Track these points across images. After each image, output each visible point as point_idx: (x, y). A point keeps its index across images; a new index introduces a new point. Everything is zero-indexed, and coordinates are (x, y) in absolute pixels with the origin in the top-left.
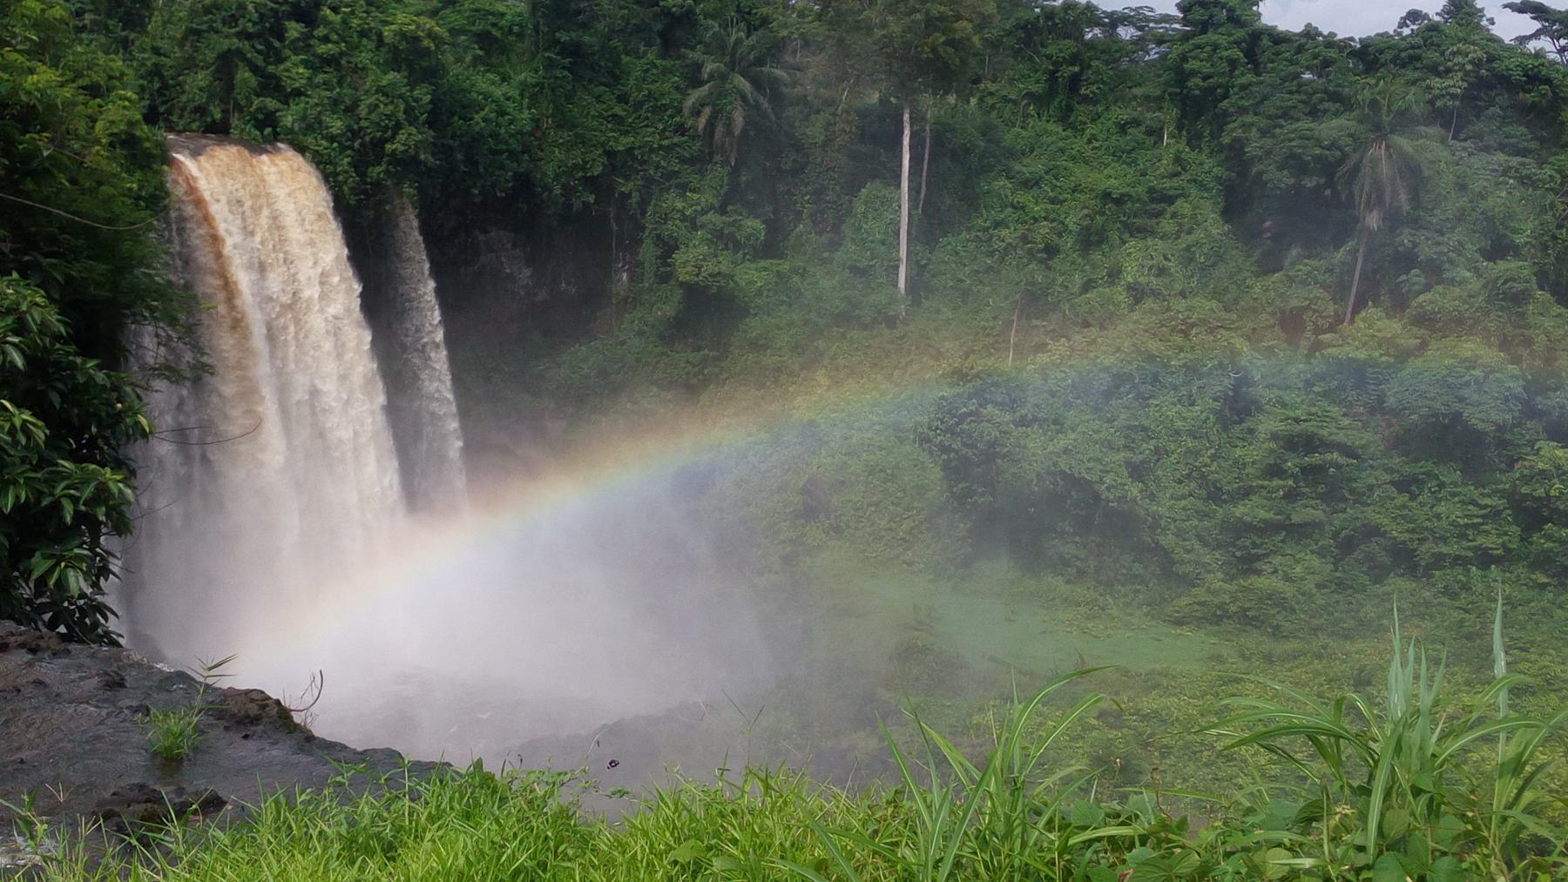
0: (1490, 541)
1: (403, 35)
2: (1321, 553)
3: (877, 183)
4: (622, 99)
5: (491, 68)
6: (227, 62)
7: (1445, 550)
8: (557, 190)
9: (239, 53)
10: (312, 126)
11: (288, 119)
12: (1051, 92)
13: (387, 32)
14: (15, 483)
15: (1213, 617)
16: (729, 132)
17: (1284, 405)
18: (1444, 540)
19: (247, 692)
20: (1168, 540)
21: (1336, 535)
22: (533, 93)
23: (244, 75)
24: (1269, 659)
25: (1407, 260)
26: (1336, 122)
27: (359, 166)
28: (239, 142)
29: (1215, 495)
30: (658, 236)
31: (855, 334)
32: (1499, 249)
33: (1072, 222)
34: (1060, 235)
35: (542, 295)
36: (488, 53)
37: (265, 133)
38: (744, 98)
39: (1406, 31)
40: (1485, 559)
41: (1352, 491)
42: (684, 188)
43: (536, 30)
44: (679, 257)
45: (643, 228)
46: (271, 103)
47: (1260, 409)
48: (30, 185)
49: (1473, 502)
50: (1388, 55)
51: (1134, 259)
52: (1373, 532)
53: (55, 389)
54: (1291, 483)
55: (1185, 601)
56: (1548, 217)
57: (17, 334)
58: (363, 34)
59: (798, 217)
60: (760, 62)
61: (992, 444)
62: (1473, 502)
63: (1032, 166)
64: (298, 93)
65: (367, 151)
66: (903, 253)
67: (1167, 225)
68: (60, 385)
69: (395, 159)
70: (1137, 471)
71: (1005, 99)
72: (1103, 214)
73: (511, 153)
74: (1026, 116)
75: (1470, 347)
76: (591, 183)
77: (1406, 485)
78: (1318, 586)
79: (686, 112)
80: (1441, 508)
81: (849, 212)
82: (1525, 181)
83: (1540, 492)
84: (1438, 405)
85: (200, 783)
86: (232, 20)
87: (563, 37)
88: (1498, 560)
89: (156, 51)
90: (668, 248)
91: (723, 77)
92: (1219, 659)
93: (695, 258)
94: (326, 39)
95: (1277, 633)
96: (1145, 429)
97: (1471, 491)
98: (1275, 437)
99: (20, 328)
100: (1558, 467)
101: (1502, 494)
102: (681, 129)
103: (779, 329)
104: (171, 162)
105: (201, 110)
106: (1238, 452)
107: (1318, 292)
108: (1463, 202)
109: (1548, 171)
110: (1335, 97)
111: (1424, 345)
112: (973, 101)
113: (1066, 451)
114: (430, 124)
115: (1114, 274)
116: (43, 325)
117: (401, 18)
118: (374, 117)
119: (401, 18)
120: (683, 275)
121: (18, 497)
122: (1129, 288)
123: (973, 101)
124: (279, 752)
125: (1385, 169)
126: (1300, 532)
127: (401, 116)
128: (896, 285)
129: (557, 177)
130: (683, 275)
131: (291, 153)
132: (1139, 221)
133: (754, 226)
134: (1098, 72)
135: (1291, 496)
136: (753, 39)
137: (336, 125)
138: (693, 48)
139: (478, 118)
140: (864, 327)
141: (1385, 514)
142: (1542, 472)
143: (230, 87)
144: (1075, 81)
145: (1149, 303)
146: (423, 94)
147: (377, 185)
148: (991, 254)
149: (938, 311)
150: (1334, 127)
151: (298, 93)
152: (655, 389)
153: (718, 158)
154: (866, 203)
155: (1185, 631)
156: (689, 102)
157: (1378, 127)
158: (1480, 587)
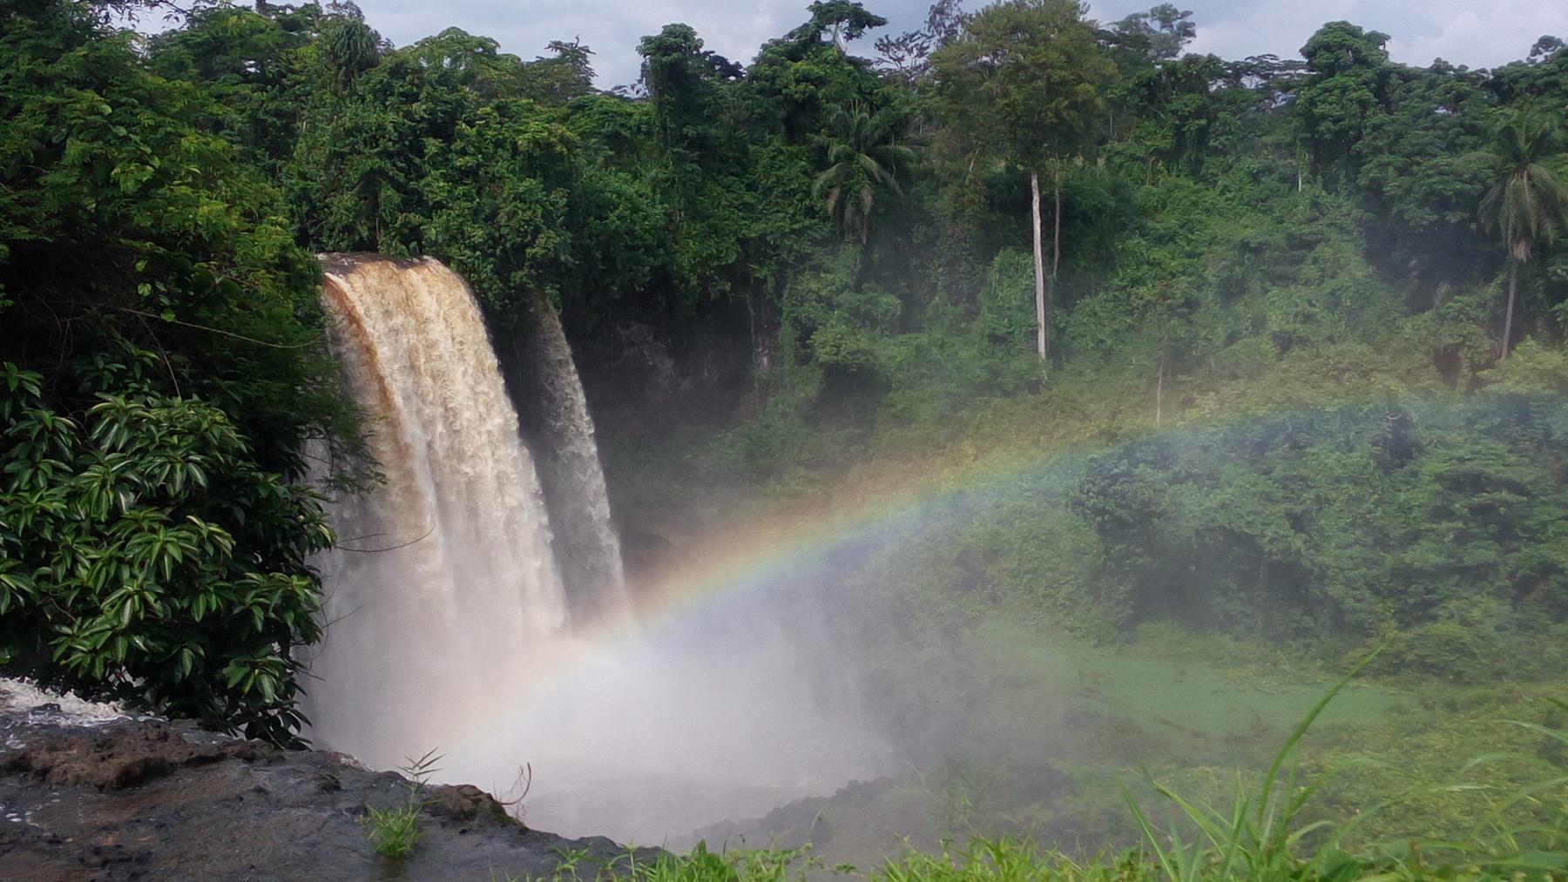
1: (537, 143)
2: (1499, 594)
3: (1010, 249)
4: (751, 187)
5: (622, 167)
6: (370, 181)
8: (694, 281)
9: (382, 172)
11: (432, 232)
12: (1179, 148)
13: (521, 141)
14: (206, 592)
15: (1393, 667)
17: (1446, 445)
20: (1337, 591)
21: (1511, 575)
22: (664, 189)
23: (387, 193)
26: (1473, 155)
27: (502, 271)
29: (1382, 541)
30: (796, 319)
31: (997, 401)
33: (1211, 274)
34: (1199, 288)
35: (686, 385)
36: (619, 154)
37: (412, 248)
38: (871, 176)
41: (1524, 529)
42: (818, 269)
43: (664, 127)
44: (817, 338)
45: (780, 312)
46: (415, 218)
47: (1421, 450)
48: (203, 312)
51: (1277, 308)
53: (241, 505)
54: (1460, 524)
55: (1359, 652)
57: (199, 453)
58: (498, 144)
59: (933, 290)
60: (885, 140)
61: (1146, 504)
63: (1170, 221)
64: (440, 206)
65: (509, 257)
66: (1041, 319)
67: (1309, 271)
68: (244, 500)
69: (536, 263)
70: (1298, 522)
71: (1134, 158)
72: (1242, 264)
74: (1155, 172)
76: (726, 271)
78: (1498, 629)
79: (815, 194)
81: (983, 282)
86: (373, 141)
87: (690, 131)
89: (303, 176)
90: (806, 331)
91: (849, 158)
92: (1399, 709)
93: (832, 338)
94: (463, 152)
95: (1459, 679)
96: (1303, 479)
98: (1439, 478)
99: (203, 446)
102: (811, 212)
103: (922, 401)
104: (320, 279)
105: (349, 229)
106: (1402, 497)
107: (1472, 328)
110: (1472, 130)
112: (1101, 162)
113: (1223, 506)
115: (1259, 325)
116: (223, 438)
117: (533, 126)
118: (512, 223)
119: (533, 126)
120: (823, 354)
121: (208, 608)
122: (1277, 336)
123: (1101, 162)
125: (1528, 197)
126: (1474, 575)
127: (539, 221)
128: (1036, 351)
129: (693, 269)
130: (823, 354)
131: (434, 265)
132: (1279, 269)
134: (1225, 124)
135: (1462, 538)
136: (877, 119)
137: (478, 234)
138: (818, 132)
139: (612, 217)
140: (1006, 394)
143: (375, 205)
144: (1203, 133)
145: (1296, 351)
146: (559, 197)
147: (521, 288)
148: (1131, 313)
149: (1080, 374)
150: (1476, 159)
151: (440, 206)
152: (802, 471)
154: (1000, 271)
155: (1363, 683)
156: (817, 186)
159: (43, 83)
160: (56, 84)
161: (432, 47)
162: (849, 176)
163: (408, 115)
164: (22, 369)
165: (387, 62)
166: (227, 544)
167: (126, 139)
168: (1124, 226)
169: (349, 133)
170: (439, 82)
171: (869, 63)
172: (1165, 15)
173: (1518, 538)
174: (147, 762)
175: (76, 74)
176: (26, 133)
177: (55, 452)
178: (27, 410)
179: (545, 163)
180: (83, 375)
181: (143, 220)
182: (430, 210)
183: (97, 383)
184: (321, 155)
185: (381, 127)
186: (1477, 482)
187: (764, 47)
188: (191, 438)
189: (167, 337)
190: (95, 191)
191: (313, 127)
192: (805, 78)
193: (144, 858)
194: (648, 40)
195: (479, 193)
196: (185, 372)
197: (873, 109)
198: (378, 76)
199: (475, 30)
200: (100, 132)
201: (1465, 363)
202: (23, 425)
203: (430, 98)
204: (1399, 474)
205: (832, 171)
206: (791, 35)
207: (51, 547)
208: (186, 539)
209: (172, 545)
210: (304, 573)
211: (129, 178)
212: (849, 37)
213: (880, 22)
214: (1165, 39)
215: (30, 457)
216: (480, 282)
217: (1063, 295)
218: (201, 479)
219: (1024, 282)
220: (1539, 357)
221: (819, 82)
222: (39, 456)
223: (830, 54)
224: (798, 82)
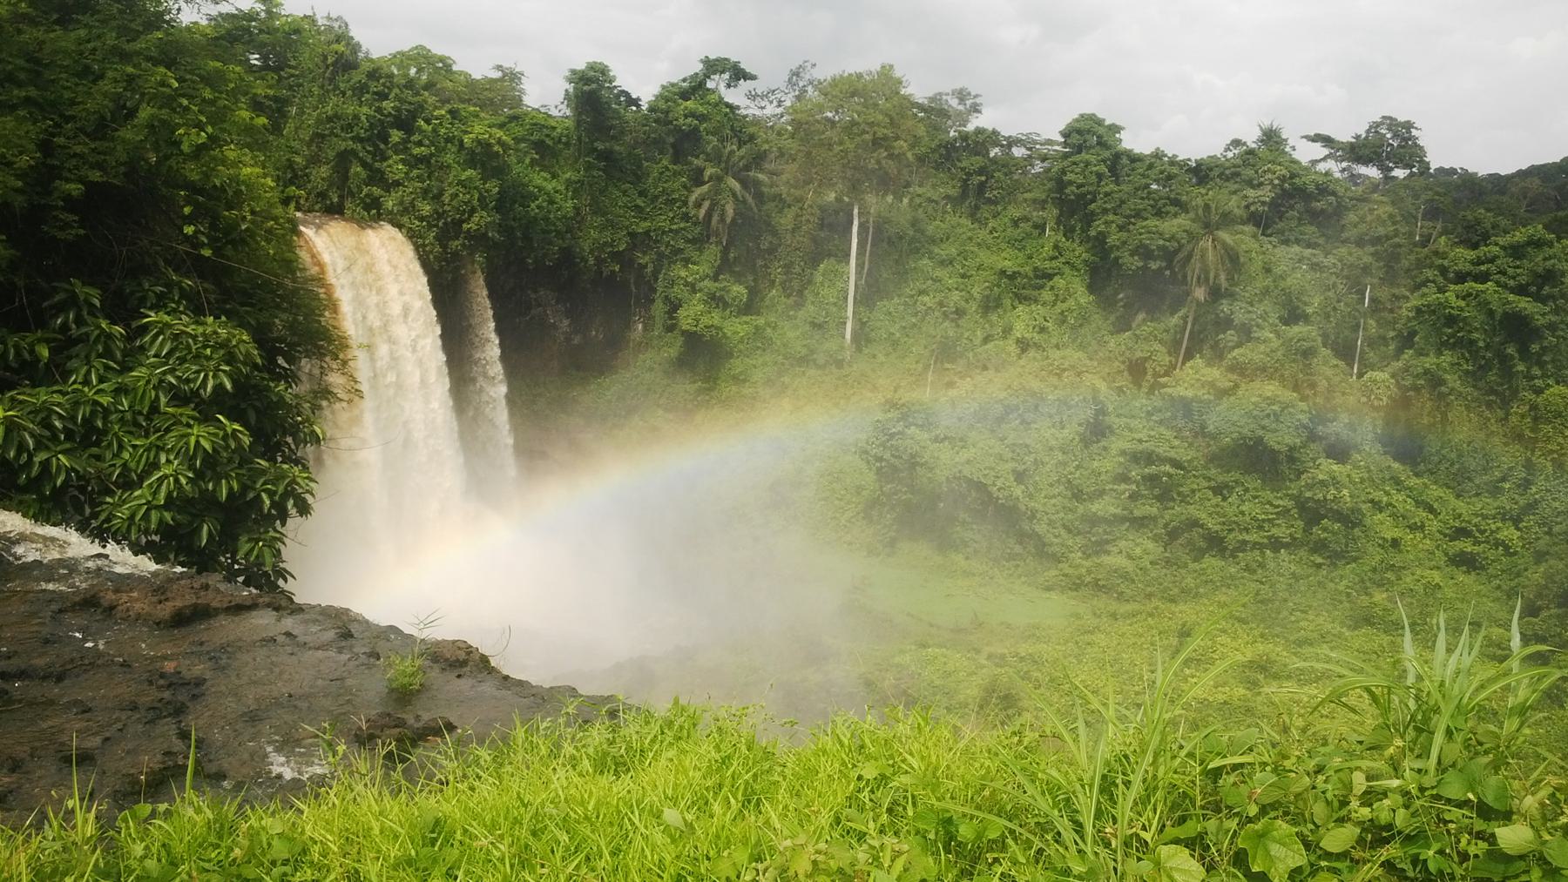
0: (1281, 531)
1: (479, 142)
2: (1156, 539)
3: (832, 260)
4: (642, 194)
5: (544, 168)
6: (344, 158)
7: (1247, 538)
8: (591, 261)
9: (354, 153)
10: (408, 209)
11: (390, 204)
15: (1076, 585)
16: (722, 220)
18: (1247, 530)
19: (454, 642)
20: (1041, 528)
21: (1166, 526)
22: (576, 188)
24: (1114, 616)
25: (1225, 324)
26: (1175, 222)
27: (442, 239)
28: (351, 220)
31: (812, 372)
32: (1293, 316)
34: (967, 301)
35: (577, 340)
36: (542, 157)
37: (372, 213)
38: (734, 195)
39: (1230, 155)
40: (1276, 545)
41: (1179, 494)
42: (687, 261)
44: (681, 313)
45: (655, 291)
46: (376, 191)
47: (1112, 432)
48: (229, 251)
50: (1216, 172)
51: (1022, 320)
52: (1194, 523)
53: (254, 407)
55: (1054, 572)
56: (1331, 294)
58: (448, 140)
60: (747, 168)
61: (912, 456)
64: (397, 184)
65: (450, 230)
67: (1046, 295)
68: (258, 404)
69: (469, 235)
70: (1020, 477)
71: (930, 200)
72: (999, 286)
73: (558, 232)
74: (945, 212)
75: (1271, 388)
76: (617, 256)
77: (1219, 490)
81: (810, 282)
82: (1315, 267)
83: (1320, 496)
84: (1245, 431)
85: (427, 714)
86: (349, 127)
87: (600, 146)
88: (1286, 546)
90: (674, 307)
91: (719, 179)
92: (1078, 616)
93: (692, 313)
94: (420, 144)
96: (1027, 446)
98: (1123, 453)
99: (230, 359)
101: (1292, 497)
102: (686, 217)
104: (299, 234)
105: (322, 195)
107: (1157, 346)
108: (1268, 282)
109: (1331, 259)
110: (1176, 202)
111: (1237, 386)
112: (906, 201)
113: (968, 462)
114: (498, 209)
115: (1007, 331)
116: (248, 354)
117: (478, 129)
119: (478, 129)
121: (230, 489)
122: (1018, 341)
123: (906, 201)
124: (488, 687)
126: (1140, 523)
127: (475, 202)
131: (389, 227)
133: (739, 290)
135: (1134, 497)
136: (743, 150)
137: (426, 208)
138: (697, 157)
140: (819, 367)
141: (1205, 511)
142: (1322, 482)
144: (982, 187)
145: (1032, 353)
146: (493, 187)
147: (455, 254)
148: (916, 315)
149: (874, 356)
150: (1175, 225)
151: (397, 184)
152: (660, 412)
153: (713, 239)
155: (1053, 595)
156: (693, 198)
157: (1207, 226)
158: (1272, 565)
159: (125, 57)
160: (135, 60)
161: (403, 59)
162: (718, 193)
163: (379, 110)
164: (84, 284)
165: (366, 67)
166: (246, 441)
167: (186, 109)
168: (917, 250)
169: (329, 119)
170: (406, 87)
171: (738, 108)
172: (962, 95)
173: (1174, 500)
174: (195, 606)
175: (154, 53)
176: (105, 95)
177: (108, 353)
178: (89, 319)
179: (484, 158)
180: (132, 293)
181: (192, 172)
182: (390, 186)
183: (142, 301)
184: (306, 135)
185: (356, 117)
186: (1150, 458)
187: (663, 87)
188: (222, 352)
189: (200, 267)
190: (156, 149)
191: (301, 112)
192: (693, 115)
193: (200, 682)
194: (574, 72)
195: (429, 177)
196: (212, 297)
197: (741, 144)
198: (358, 77)
199: (438, 49)
200: (169, 102)
201: (1150, 372)
202: (84, 330)
203: (397, 98)
204: (1094, 448)
205: (705, 188)
206: (684, 80)
207: (104, 432)
208: (215, 435)
209: (201, 436)
210: (297, 462)
211: (192, 138)
212: (729, 86)
213: (753, 78)
214: (960, 113)
215: (87, 357)
216: (424, 245)
217: (869, 295)
218: (229, 386)
219: (840, 285)
221: (702, 118)
222: (93, 355)
223: (712, 98)
224: (686, 116)
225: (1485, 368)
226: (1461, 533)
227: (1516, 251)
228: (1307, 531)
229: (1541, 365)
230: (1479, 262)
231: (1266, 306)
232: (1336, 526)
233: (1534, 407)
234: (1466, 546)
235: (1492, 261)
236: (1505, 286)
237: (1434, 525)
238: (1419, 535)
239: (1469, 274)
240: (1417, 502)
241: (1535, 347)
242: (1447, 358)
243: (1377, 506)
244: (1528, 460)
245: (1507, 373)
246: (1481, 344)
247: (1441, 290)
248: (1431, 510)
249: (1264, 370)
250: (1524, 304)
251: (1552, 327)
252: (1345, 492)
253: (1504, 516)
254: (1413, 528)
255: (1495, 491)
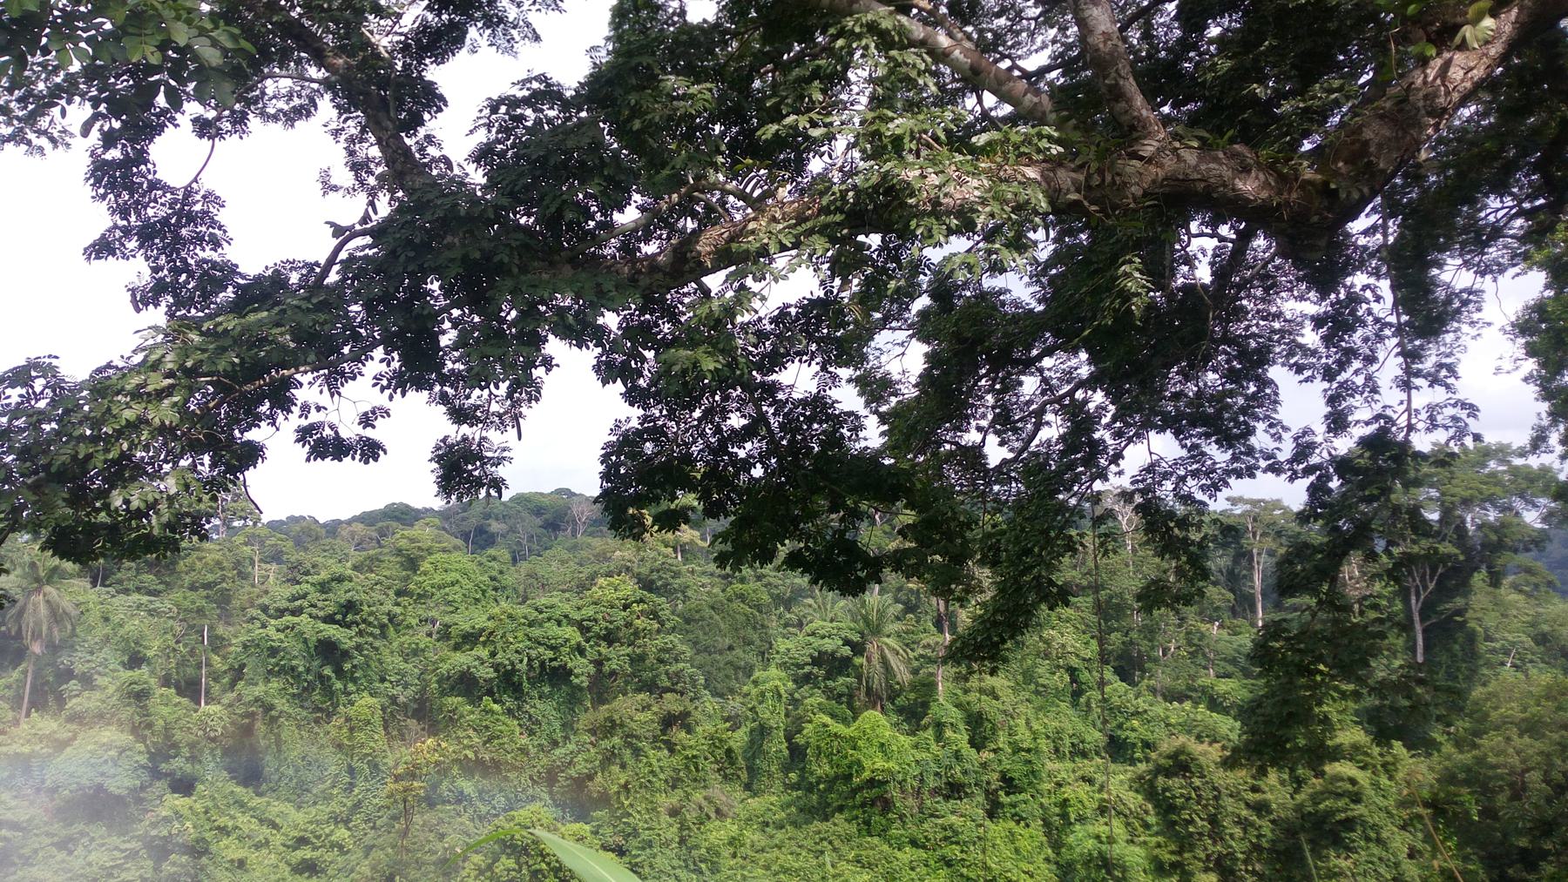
25: (68, 674)
32: (135, 660)
41: (21, 857)
49: (117, 848)
56: (169, 636)
62: (117, 848)
77: (65, 845)
80: (93, 857)
82: (152, 613)
83: (165, 833)
84: (85, 781)
97: (115, 840)
100: (176, 813)
101: (139, 838)
108: (108, 630)
111: (74, 738)
125: (43, 610)
142: (165, 818)
157: (38, 580)
173: (14, 864)
220: (40, 725)
225: (309, 689)
226: (302, 841)
227: (324, 587)
228: (157, 869)
229: (354, 680)
230: (294, 599)
231: (106, 653)
232: (184, 859)
233: (348, 719)
234: (307, 853)
235: (304, 596)
236: (316, 617)
237: (277, 839)
238: (264, 851)
239: (287, 609)
240: (261, 821)
241: (347, 666)
242: (275, 684)
243: (223, 831)
244: (350, 766)
245: (329, 693)
246: (301, 669)
247: (264, 626)
248: (274, 826)
249: (101, 716)
250: (332, 631)
251: (359, 648)
252: (188, 824)
253: (336, 819)
254: (258, 846)
255: (328, 798)
